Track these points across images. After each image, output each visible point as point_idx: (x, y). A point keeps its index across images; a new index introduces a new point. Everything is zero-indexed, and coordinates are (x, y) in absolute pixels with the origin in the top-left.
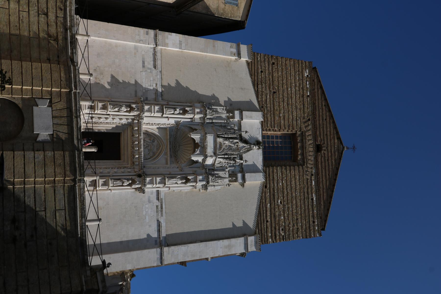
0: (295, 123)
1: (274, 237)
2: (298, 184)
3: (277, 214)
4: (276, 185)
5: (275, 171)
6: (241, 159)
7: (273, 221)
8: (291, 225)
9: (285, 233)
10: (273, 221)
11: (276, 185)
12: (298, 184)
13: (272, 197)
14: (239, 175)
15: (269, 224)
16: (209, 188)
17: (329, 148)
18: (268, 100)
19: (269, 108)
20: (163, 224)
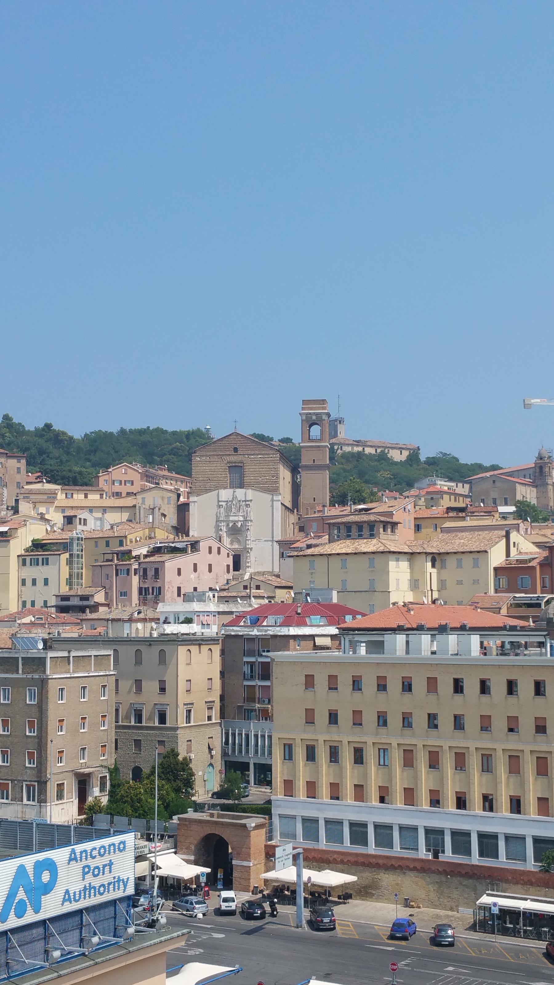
0: (223, 468)
1: (276, 483)
2: (252, 467)
3: (266, 481)
4: (253, 481)
5: (246, 481)
6: (240, 501)
7: (268, 483)
8: (272, 472)
9: (275, 476)
10: (268, 483)
11: (253, 481)
12: (252, 467)
13: (258, 483)
14: (247, 503)
15: (270, 486)
16: (252, 519)
17: (236, 442)
18: (214, 484)
19: (217, 484)
20: (265, 539)
